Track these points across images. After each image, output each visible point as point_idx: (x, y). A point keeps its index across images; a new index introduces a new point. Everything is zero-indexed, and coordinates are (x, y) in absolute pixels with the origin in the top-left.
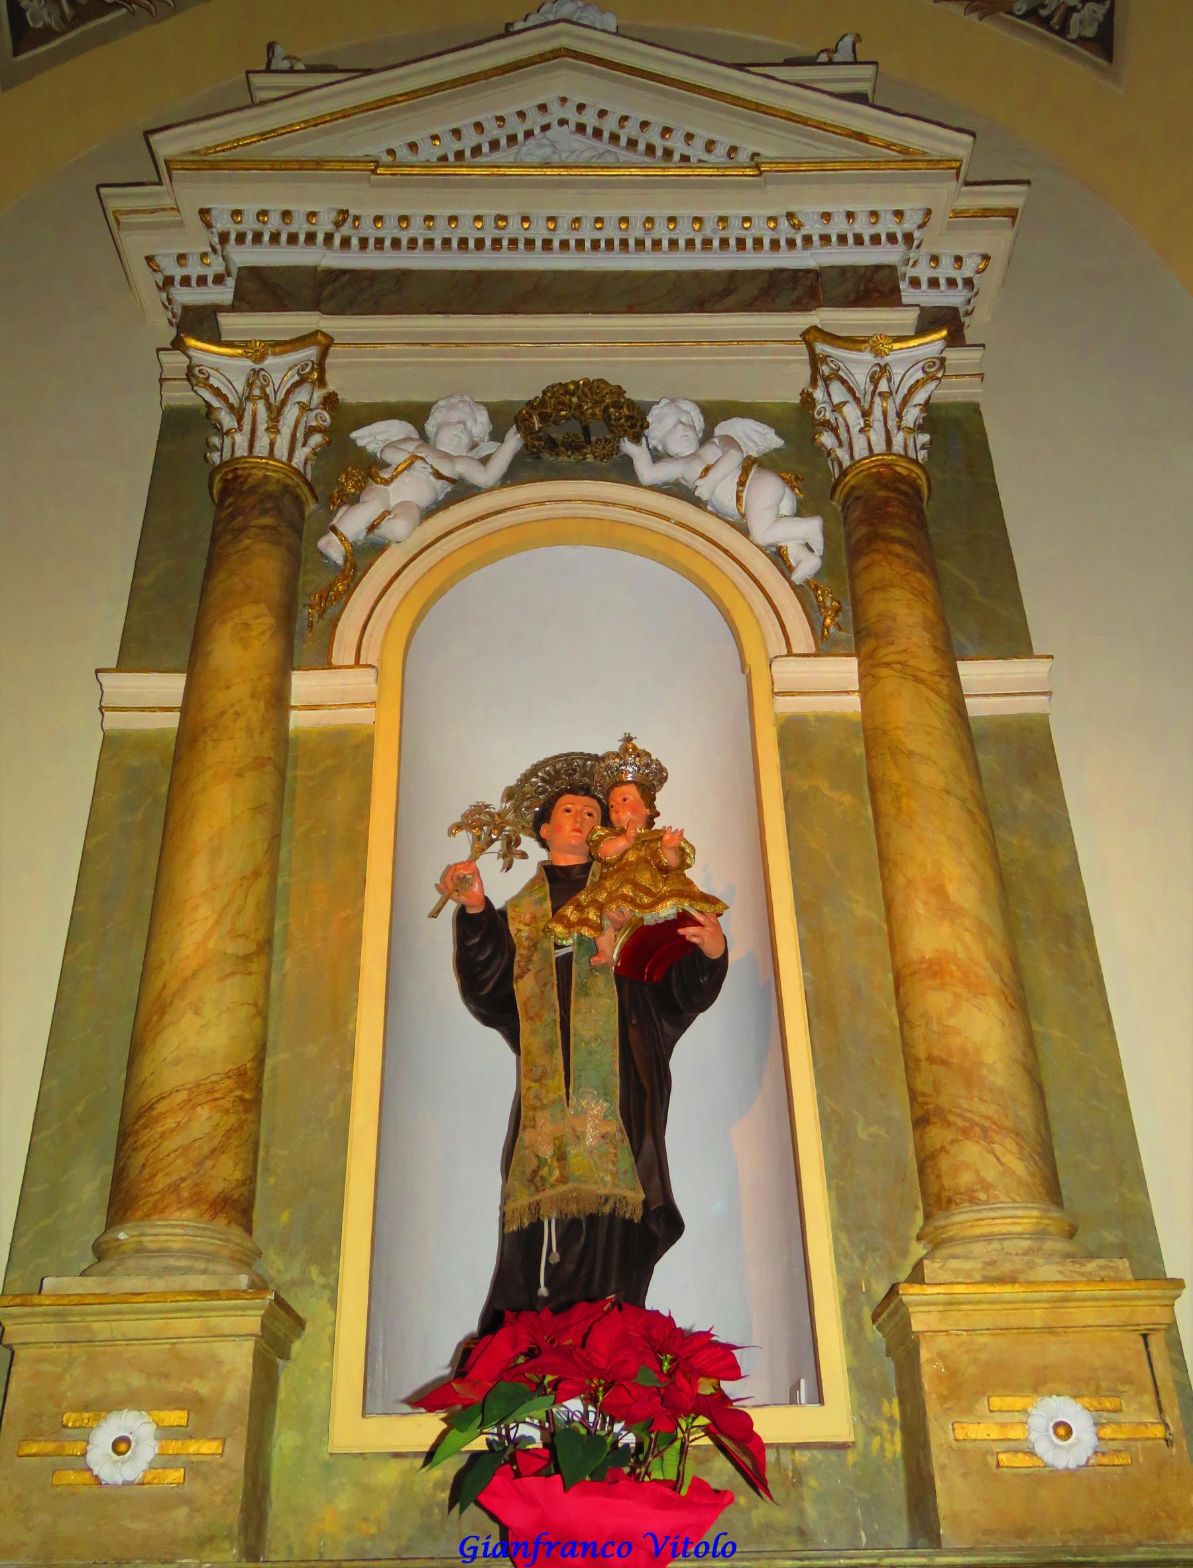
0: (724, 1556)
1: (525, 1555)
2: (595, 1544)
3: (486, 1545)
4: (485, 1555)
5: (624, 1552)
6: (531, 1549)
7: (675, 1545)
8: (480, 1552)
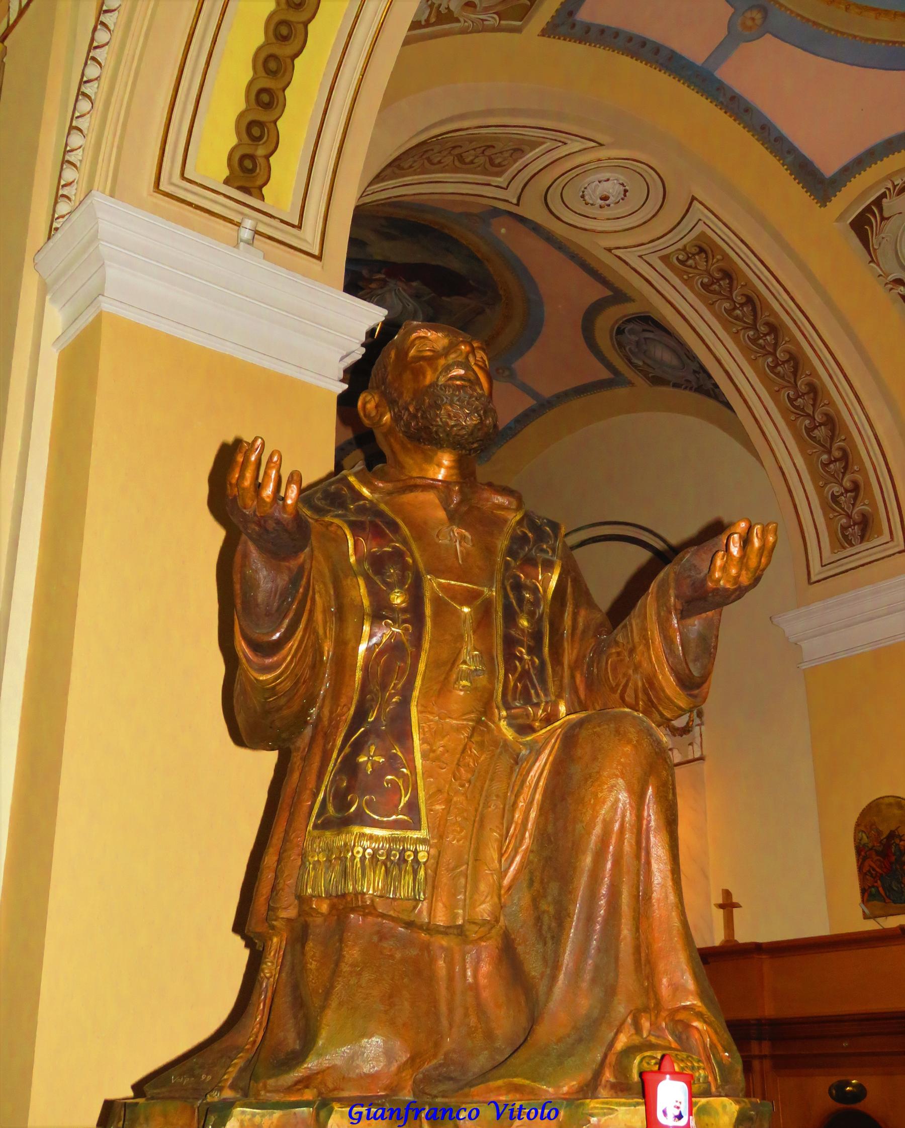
0: (549, 1119)
4: (368, 1118)
6: (403, 1112)
7: (512, 1110)
8: (365, 1113)
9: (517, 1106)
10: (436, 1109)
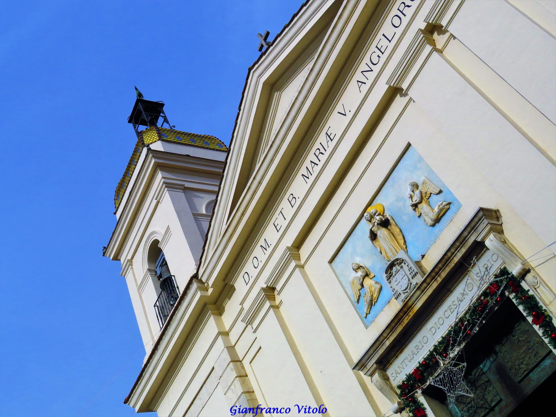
1: (253, 413)
2: (277, 409)
3: (240, 409)
5: (288, 411)
6: (255, 411)
7: (305, 409)
9: (308, 407)
10: (270, 409)
